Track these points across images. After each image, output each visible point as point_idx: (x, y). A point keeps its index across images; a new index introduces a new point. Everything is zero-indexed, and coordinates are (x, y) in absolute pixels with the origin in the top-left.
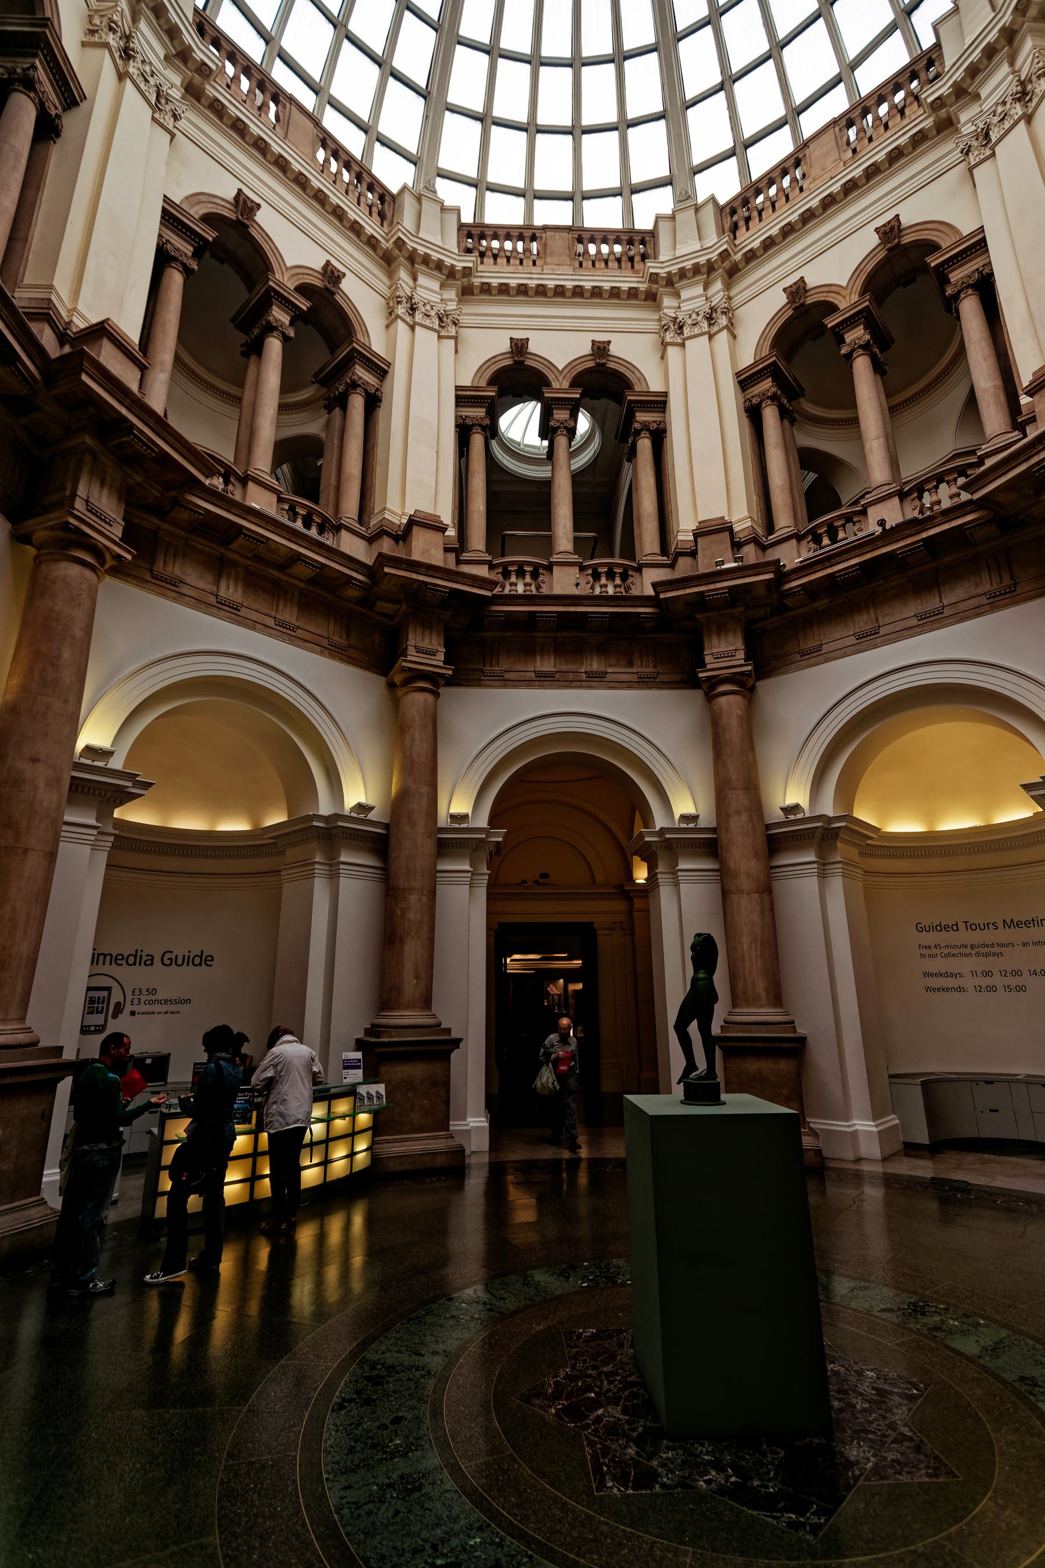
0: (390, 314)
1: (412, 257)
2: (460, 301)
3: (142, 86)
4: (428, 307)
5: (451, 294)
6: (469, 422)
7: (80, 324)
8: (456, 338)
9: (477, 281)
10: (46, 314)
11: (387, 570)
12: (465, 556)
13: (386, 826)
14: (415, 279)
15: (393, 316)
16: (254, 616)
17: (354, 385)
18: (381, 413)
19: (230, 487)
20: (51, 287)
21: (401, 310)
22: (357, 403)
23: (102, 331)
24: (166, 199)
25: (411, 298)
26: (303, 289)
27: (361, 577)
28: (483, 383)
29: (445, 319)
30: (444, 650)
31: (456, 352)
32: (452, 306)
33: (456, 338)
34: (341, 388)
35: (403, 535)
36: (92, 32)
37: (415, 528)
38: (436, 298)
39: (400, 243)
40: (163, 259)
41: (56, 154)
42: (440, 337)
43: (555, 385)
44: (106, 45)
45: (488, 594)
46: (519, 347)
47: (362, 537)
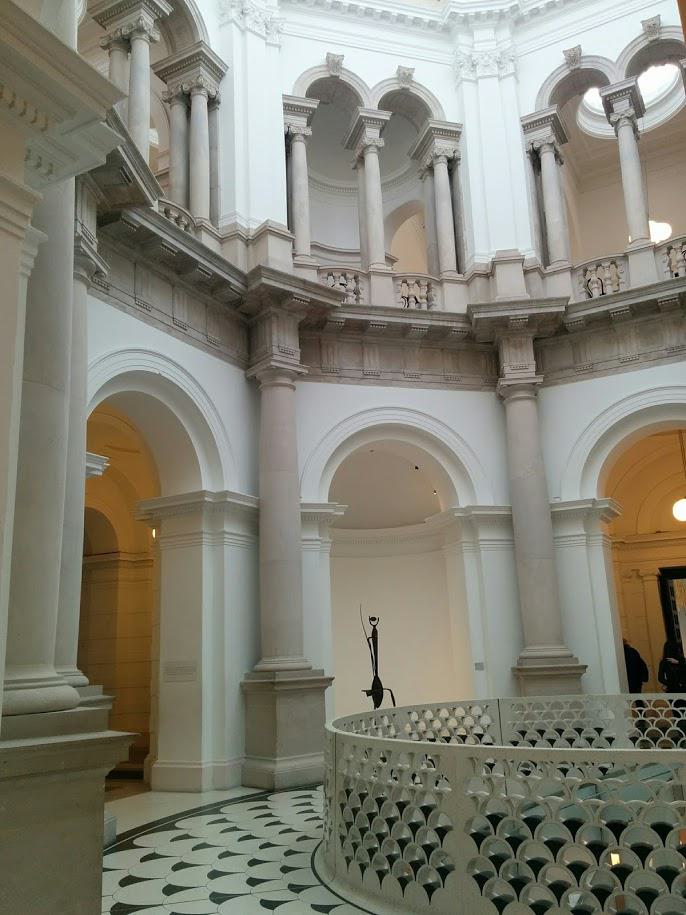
0: (457, 78)
1: (466, 20)
2: (513, 33)
3: (256, 29)
4: (486, 58)
5: (506, 33)
6: (536, 146)
7: (254, 227)
8: (515, 74)
9: (525, 11)
10: (233, 236)
11: (475, 316)
12: (550, 269)
13: (510, 509)
14: (472, 35)
15: (458, 81)
16: (390, 376)
17: (437, 157)
18: (461, 170)
19: (360, 285)
20: (235, 214)
21: (464, 73)
22: (441, 170)
23: (266, 231)
24: (285, 97)
25: (471, 56)
26: (387, 102)
27: (460, 325)
28: (545, 105)
29: (503, 61)
30: (534, 362)
31: (518, 82)
32: (508, 45)
33: (515, 74)
34: (428, 162)
35: (489, 275)
36: (223, 15)
37: (499, 270)
38: (492, 45)
39: (453, 16)
40: (289, 138)
41: (221, 112)
42: (500, 79)
43: (612, 80)
44: (233, 21)
45: (563, 309)
46: (574, 57)
47: (461, 282)
